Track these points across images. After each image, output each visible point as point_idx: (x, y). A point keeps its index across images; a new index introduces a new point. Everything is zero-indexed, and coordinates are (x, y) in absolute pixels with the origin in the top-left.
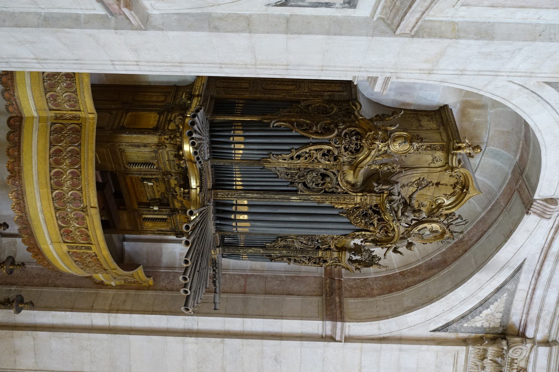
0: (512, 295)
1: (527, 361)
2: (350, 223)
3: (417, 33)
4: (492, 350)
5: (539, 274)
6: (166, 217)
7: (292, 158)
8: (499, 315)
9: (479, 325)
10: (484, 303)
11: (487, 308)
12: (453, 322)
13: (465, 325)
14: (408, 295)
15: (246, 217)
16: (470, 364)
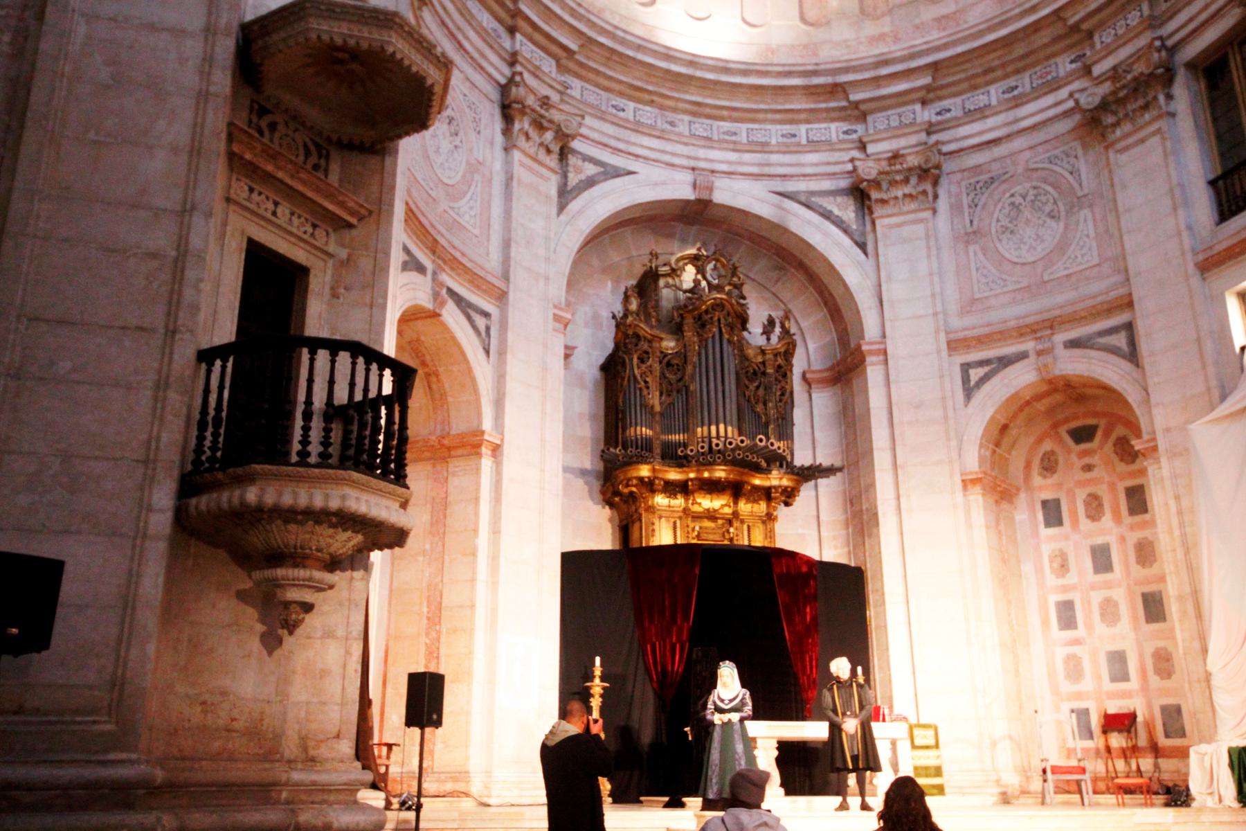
0: (813, 193)
1: (879, 160)
2: (713, 337)
3: (506, 277)
4: (875, 195)
5: (785, 176)
6: (745, 527)
7: (648, 388)
8: (839, 199)
9: (852, 215)
10: (827, 215)
11: (831, 212)
12: (852, 239)
13: (854, 227)
14: (837, 292)
15: (713, 428)
16: (896, 210)
